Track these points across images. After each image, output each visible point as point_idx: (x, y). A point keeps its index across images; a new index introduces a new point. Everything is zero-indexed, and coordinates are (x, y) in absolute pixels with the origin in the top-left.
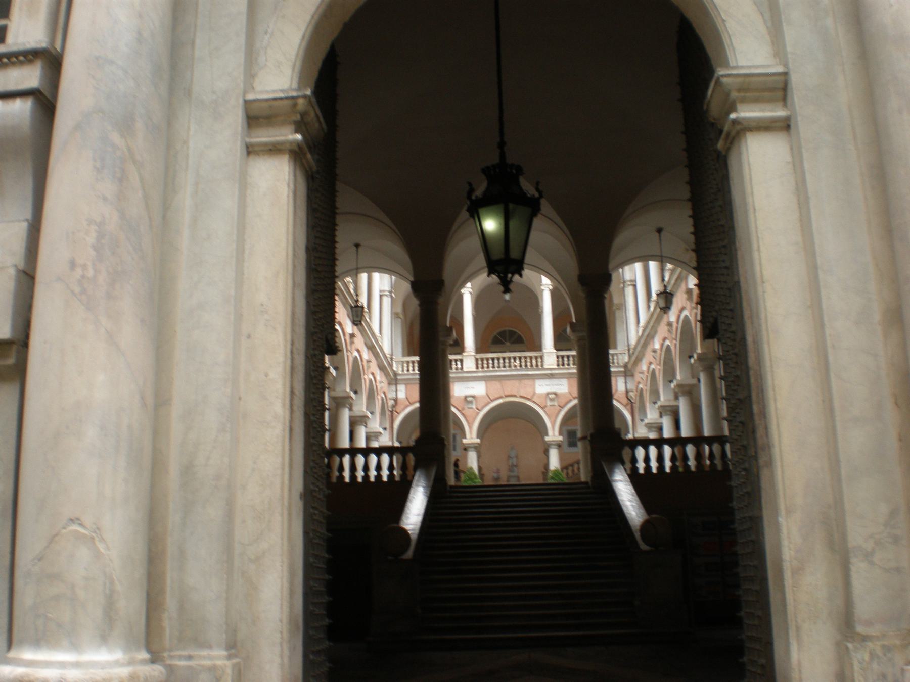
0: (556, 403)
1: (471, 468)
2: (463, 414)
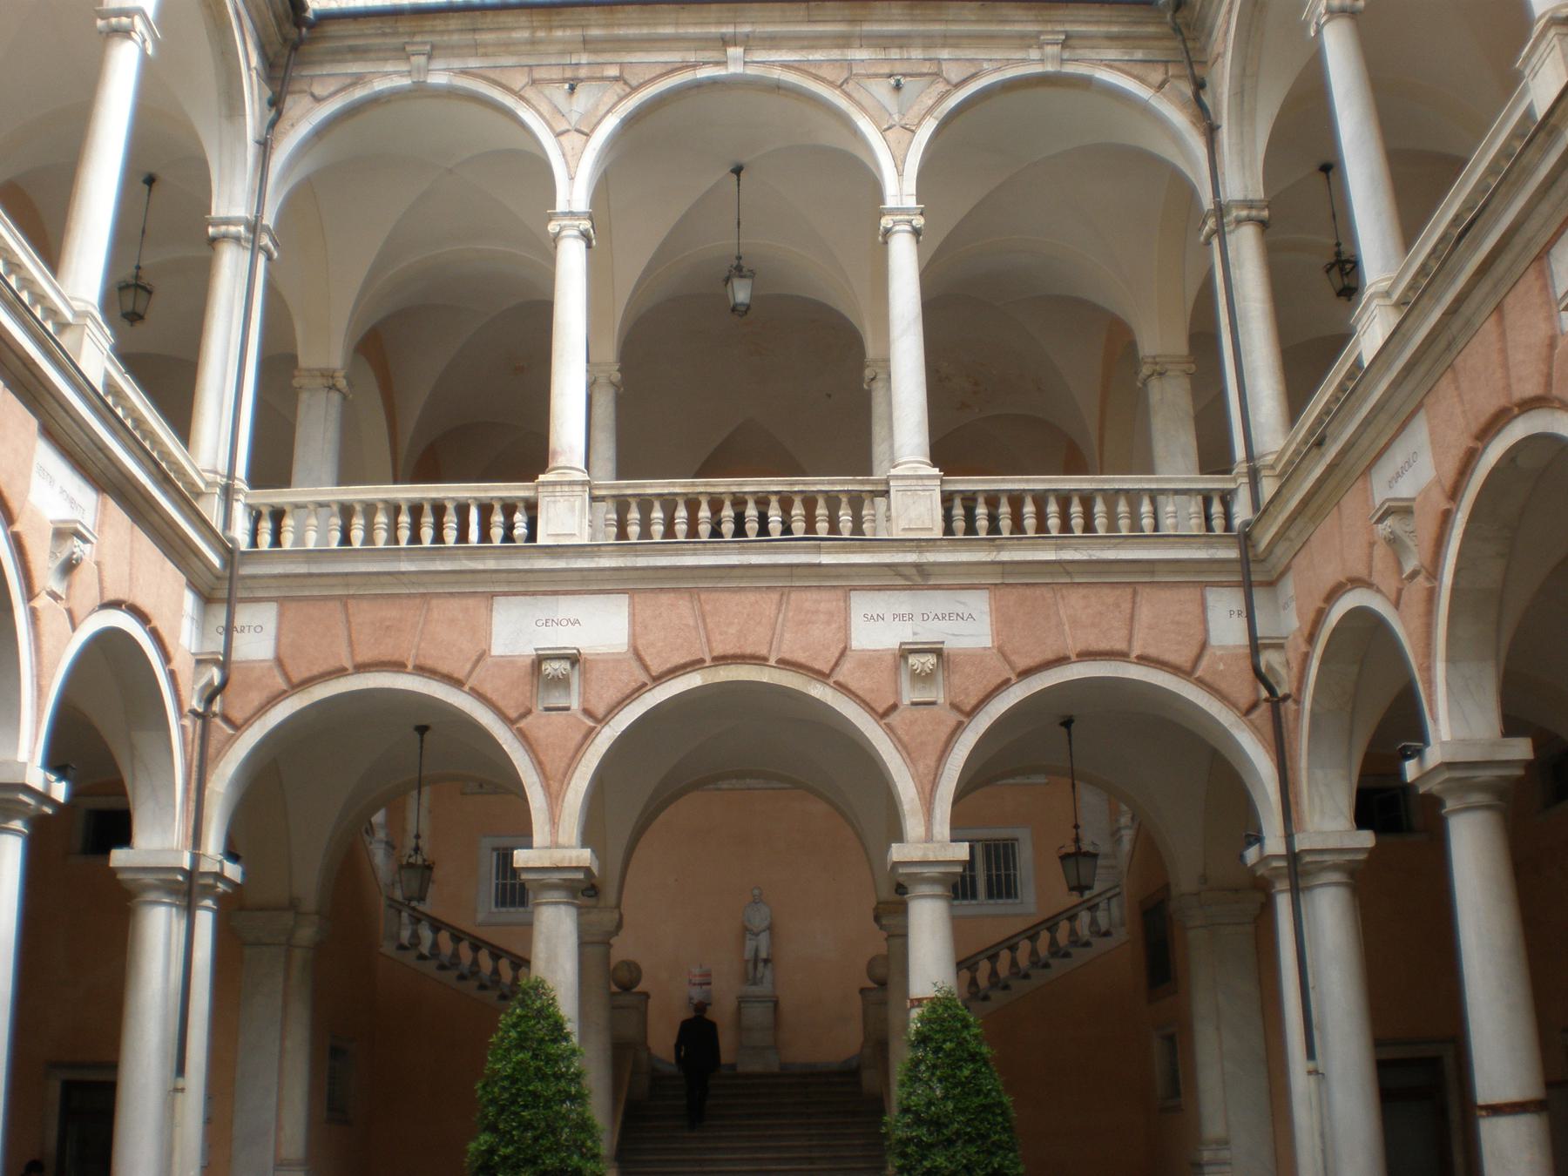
0: (938, 694)
1: (539, 988)
2: (524, 737)
